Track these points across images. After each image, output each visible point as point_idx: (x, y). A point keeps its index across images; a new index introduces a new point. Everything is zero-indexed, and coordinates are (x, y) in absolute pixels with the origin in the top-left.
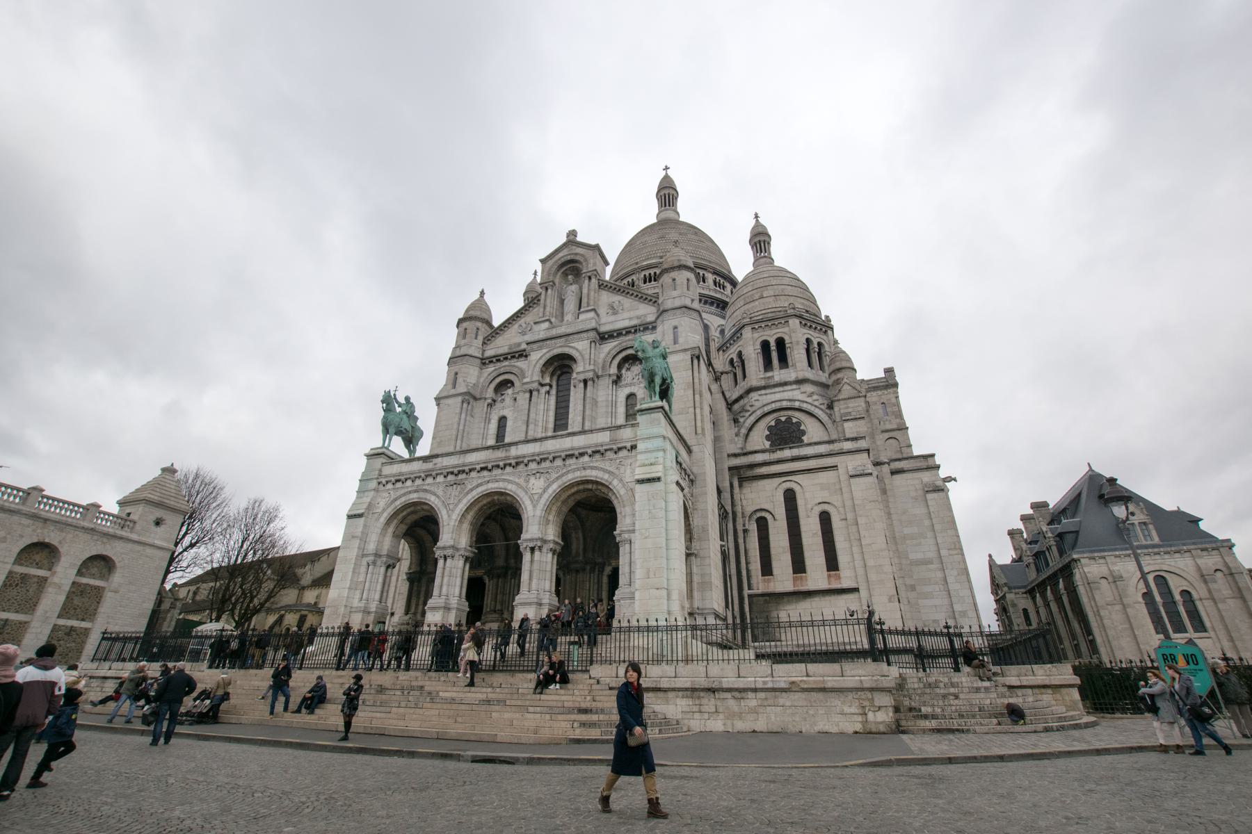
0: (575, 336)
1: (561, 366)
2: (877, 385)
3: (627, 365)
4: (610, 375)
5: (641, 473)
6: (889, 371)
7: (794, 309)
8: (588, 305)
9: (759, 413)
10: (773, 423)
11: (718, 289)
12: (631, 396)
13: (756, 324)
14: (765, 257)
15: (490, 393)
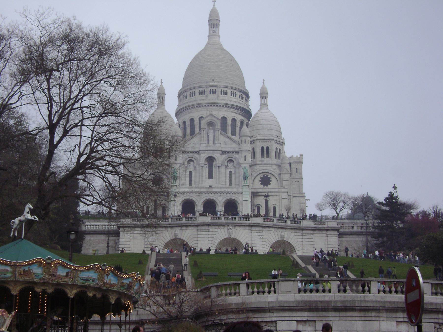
0: (216, 151)
1: (210, 160)
2: (296, 161)
3: (229, 162)
4: (225, 165)
5: (244, 199)
6: (301, 155)
7: (273, 137)
8: (218, 141)
9: (258, 173)
10: (262, 176)
11: (240, 99)
12: (230, 172)
13: (261, 141)
14: (265, 105)
15: (186, 163)
